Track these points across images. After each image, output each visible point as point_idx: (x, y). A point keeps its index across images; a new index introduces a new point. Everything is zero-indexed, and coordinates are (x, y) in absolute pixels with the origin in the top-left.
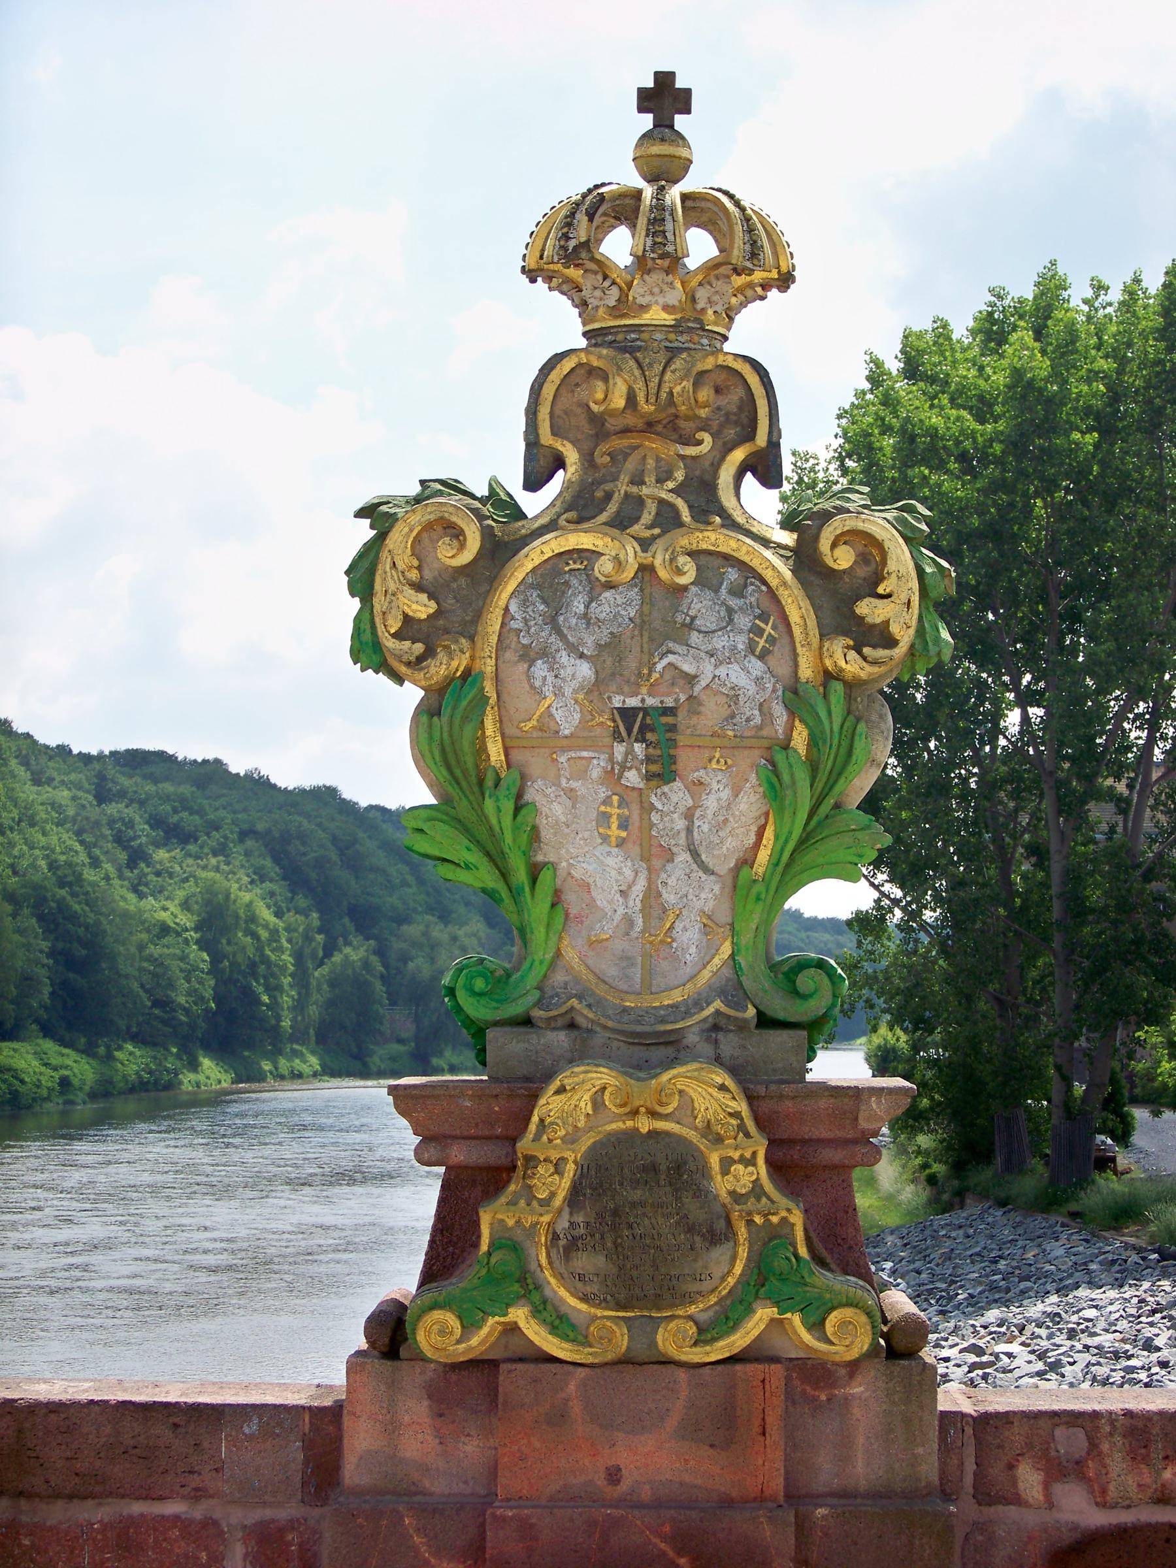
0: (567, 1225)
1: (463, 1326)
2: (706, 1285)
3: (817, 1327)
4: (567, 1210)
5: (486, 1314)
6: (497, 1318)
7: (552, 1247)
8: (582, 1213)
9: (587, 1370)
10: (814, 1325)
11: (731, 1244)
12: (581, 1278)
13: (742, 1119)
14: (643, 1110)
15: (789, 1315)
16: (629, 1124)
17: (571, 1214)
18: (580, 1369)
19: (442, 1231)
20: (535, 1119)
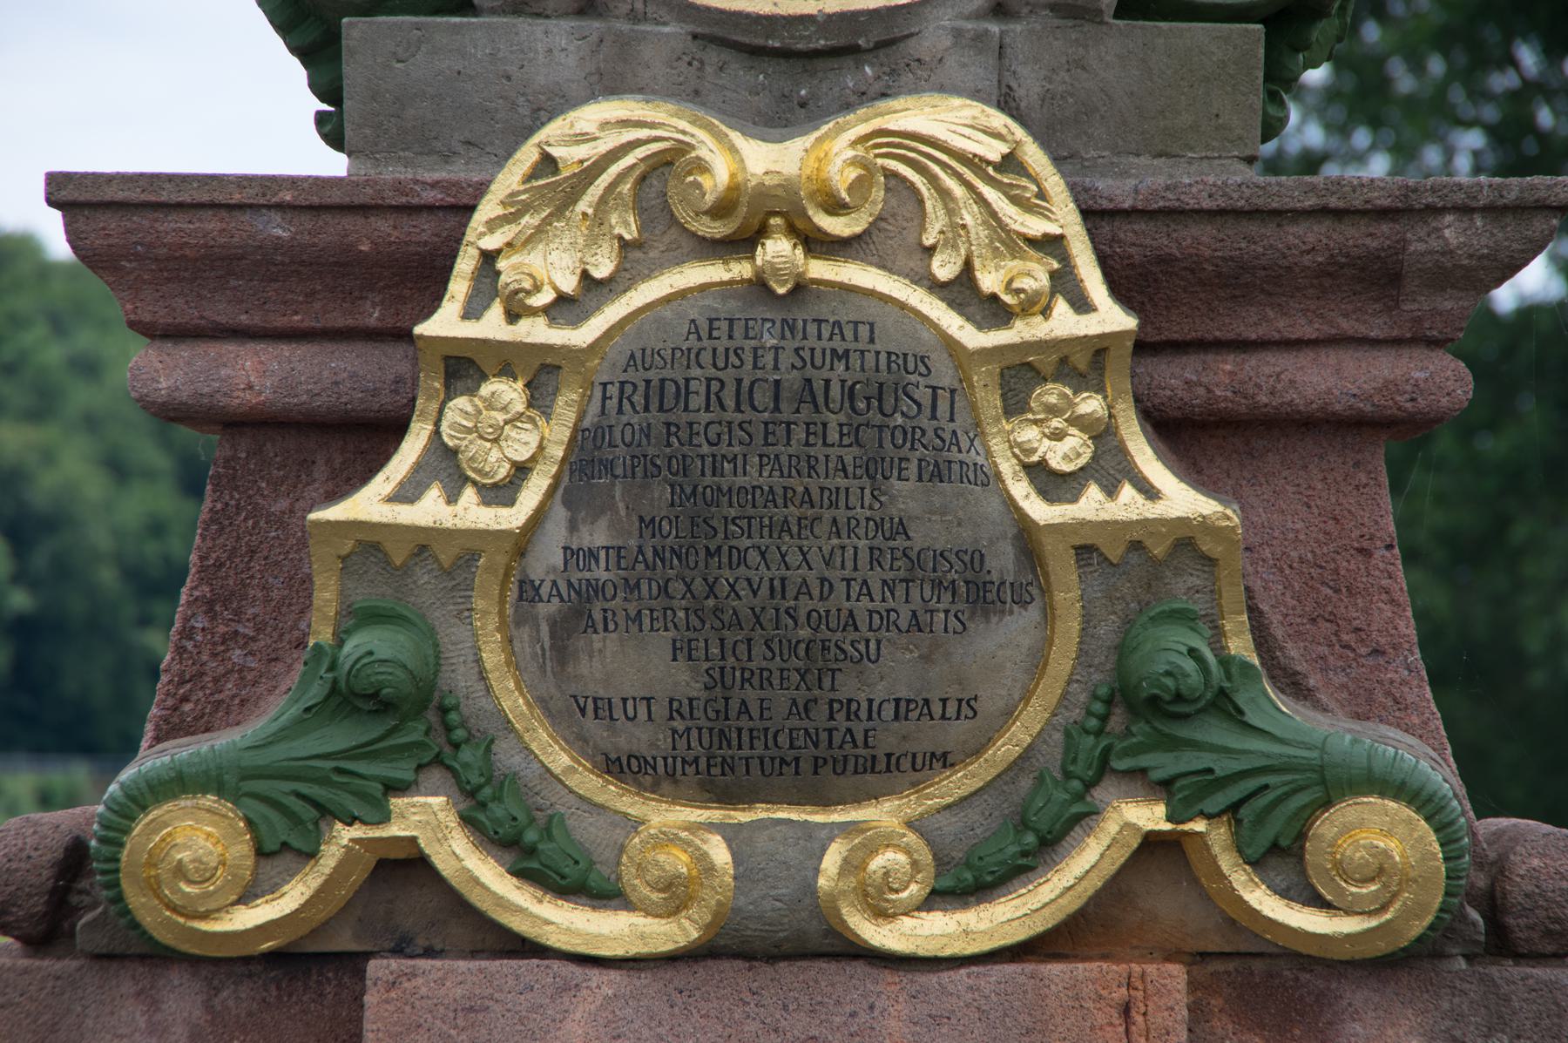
0: (558, 559)
1: (261, 853)
2: (957, 732)
3: (1282, 858)
4: (560, 513)
5: (327, 813)
6: (357, 832)
7: (518, 624)
8: (603, 523)
9: (614, 975)
10: (1275, 849)
11: (1033, 613)
12: (602, 708)
13: (1065, 259)
14: (775, 221)
15: (1199, 826)
16: (741, 270)
17: (573, 527)
18: (595, 975)
19: (210, 604)
20: (465, 264)
